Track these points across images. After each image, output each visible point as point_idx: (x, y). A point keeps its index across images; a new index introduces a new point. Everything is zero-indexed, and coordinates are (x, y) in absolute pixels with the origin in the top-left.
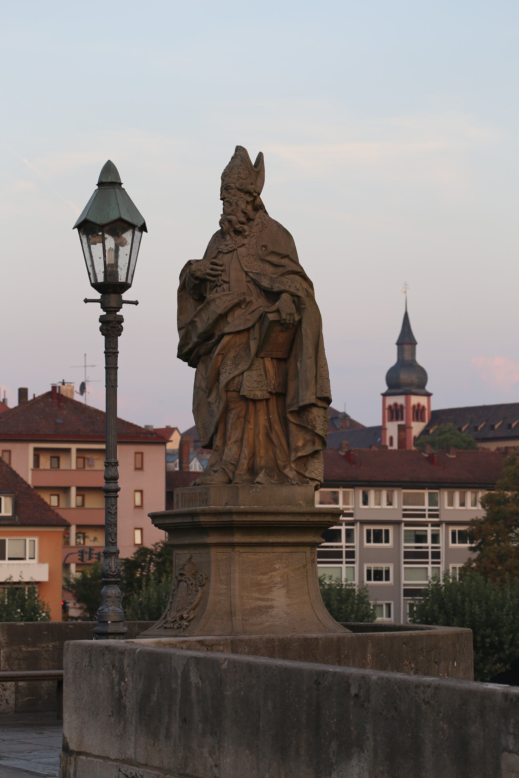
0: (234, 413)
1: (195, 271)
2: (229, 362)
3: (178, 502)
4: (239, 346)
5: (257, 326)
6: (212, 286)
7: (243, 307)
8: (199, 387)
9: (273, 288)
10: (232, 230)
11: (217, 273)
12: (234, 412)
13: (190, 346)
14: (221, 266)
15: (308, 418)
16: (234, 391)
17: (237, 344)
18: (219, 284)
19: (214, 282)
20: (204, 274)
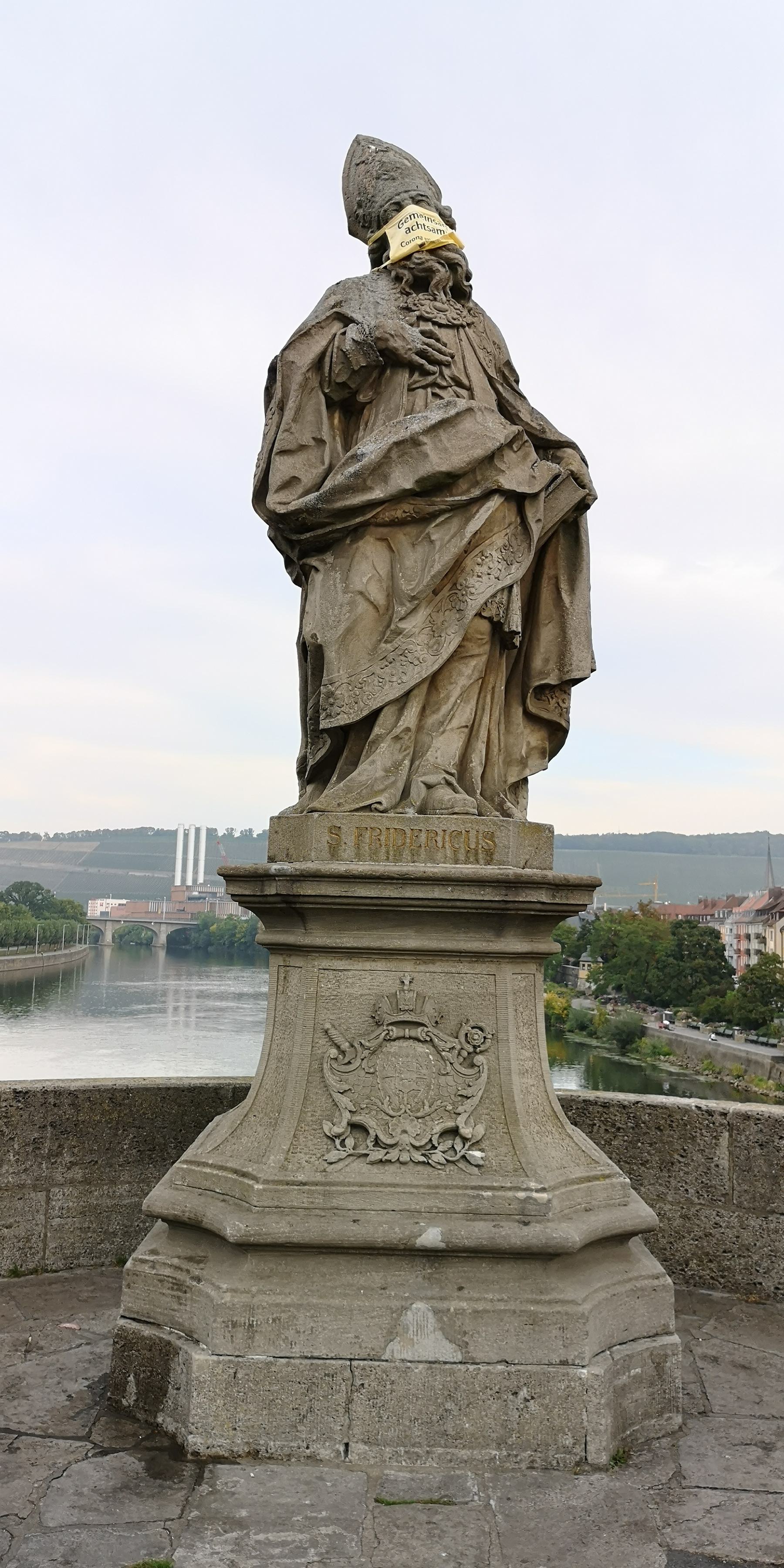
0: (475, 667)
1: (392, 335)
2: (494, 553)
3: (339, 844)
4: (509, 525)
5: (543, 495)
6: (415, 382)
7: (515, 447)
8: (361, 593)
9: (544, 432)
10: (451, 284)
11: (442, 357)
12: (473, 663)
13: (378, 494)
14: (445, 345)
15: (561, 704)
16: (490, 619)
17: (507, 521)
18: (444, 384)
19: (427, 373)
20: (410, 349)
